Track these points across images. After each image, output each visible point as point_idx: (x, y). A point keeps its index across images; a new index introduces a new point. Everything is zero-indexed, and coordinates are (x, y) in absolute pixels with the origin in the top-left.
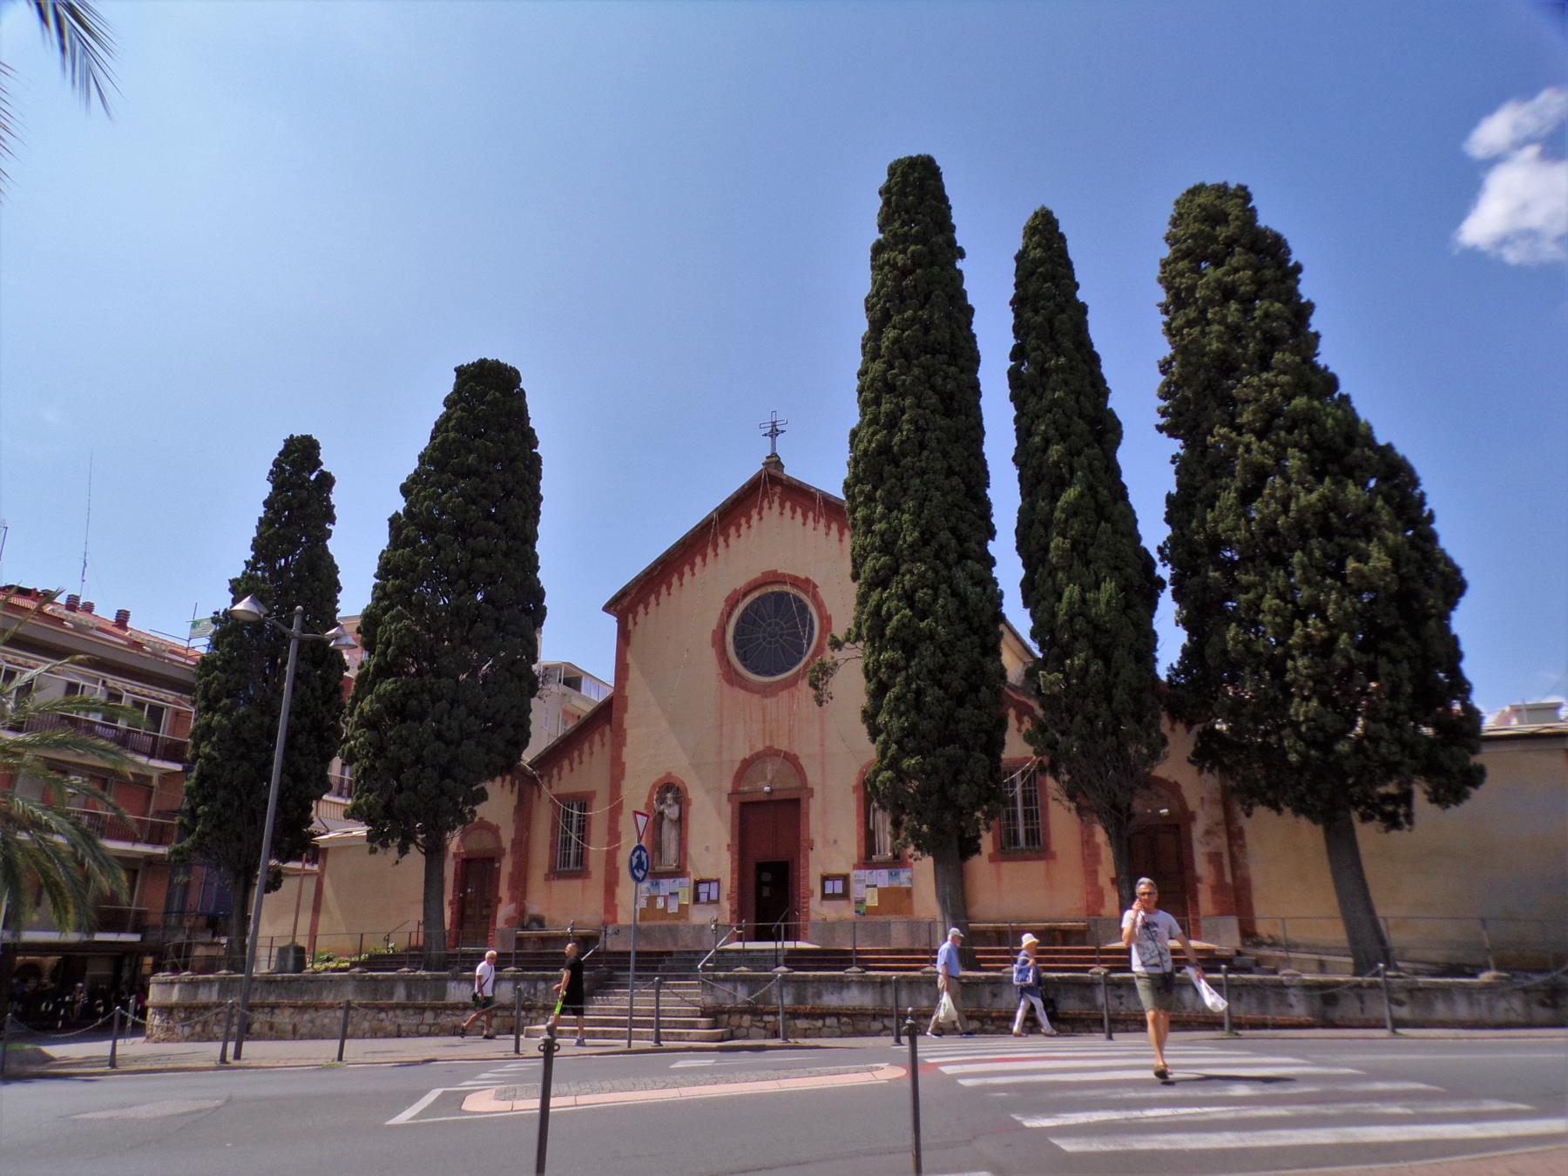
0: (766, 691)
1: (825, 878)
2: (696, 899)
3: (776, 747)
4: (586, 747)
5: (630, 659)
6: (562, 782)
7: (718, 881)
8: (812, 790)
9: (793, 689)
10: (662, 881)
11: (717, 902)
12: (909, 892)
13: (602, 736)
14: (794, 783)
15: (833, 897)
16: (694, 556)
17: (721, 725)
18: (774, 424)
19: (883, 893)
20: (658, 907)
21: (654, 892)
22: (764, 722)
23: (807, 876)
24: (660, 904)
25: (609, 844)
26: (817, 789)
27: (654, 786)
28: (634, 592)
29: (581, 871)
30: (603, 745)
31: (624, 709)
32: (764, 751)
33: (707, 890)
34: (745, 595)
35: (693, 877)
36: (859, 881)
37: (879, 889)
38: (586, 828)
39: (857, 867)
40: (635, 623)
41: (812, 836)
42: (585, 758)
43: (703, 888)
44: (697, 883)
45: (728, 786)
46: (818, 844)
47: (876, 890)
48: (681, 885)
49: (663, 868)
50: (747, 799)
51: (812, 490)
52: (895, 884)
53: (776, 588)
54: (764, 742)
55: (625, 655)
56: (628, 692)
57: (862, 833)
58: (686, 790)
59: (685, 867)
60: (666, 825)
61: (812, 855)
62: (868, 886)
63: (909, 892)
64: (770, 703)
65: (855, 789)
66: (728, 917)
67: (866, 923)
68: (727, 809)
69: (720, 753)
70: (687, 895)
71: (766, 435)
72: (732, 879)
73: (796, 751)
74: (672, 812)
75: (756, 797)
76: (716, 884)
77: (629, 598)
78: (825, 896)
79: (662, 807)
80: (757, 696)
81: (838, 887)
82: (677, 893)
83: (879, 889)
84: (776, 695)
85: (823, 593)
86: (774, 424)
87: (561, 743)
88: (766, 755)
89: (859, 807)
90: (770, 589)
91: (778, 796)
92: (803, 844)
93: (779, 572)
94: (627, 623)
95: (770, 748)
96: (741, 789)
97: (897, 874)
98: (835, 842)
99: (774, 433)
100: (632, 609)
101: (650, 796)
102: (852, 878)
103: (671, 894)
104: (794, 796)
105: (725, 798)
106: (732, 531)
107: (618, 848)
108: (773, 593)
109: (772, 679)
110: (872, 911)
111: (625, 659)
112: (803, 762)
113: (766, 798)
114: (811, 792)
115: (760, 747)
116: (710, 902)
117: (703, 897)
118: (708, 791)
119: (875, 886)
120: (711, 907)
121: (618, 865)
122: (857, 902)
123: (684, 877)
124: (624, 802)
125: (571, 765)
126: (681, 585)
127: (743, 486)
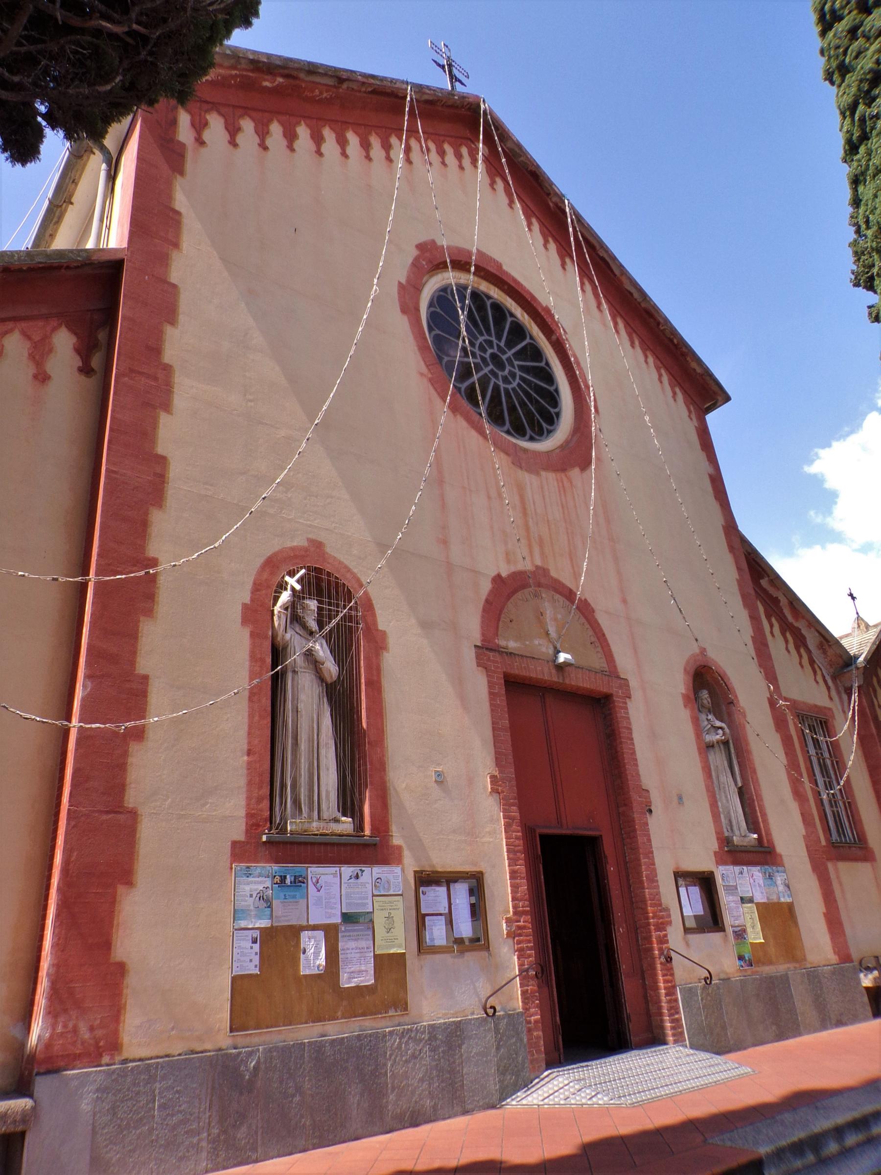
9: (563, 475)
10: (314, 871)
14: (596, 661)
20: (304, 971)
33: (443, 908)
37: (758, 905)
48: (380, 891)
50: (518, 669)
69: (445, 542)
72: (513, 875)
83: (758, 905)
98: (680, 798)
103: (348, 918)
105: (469, 655)
107: (139, 734)
113: (553, 677)
120: (471, 958)
121: (131, 799)
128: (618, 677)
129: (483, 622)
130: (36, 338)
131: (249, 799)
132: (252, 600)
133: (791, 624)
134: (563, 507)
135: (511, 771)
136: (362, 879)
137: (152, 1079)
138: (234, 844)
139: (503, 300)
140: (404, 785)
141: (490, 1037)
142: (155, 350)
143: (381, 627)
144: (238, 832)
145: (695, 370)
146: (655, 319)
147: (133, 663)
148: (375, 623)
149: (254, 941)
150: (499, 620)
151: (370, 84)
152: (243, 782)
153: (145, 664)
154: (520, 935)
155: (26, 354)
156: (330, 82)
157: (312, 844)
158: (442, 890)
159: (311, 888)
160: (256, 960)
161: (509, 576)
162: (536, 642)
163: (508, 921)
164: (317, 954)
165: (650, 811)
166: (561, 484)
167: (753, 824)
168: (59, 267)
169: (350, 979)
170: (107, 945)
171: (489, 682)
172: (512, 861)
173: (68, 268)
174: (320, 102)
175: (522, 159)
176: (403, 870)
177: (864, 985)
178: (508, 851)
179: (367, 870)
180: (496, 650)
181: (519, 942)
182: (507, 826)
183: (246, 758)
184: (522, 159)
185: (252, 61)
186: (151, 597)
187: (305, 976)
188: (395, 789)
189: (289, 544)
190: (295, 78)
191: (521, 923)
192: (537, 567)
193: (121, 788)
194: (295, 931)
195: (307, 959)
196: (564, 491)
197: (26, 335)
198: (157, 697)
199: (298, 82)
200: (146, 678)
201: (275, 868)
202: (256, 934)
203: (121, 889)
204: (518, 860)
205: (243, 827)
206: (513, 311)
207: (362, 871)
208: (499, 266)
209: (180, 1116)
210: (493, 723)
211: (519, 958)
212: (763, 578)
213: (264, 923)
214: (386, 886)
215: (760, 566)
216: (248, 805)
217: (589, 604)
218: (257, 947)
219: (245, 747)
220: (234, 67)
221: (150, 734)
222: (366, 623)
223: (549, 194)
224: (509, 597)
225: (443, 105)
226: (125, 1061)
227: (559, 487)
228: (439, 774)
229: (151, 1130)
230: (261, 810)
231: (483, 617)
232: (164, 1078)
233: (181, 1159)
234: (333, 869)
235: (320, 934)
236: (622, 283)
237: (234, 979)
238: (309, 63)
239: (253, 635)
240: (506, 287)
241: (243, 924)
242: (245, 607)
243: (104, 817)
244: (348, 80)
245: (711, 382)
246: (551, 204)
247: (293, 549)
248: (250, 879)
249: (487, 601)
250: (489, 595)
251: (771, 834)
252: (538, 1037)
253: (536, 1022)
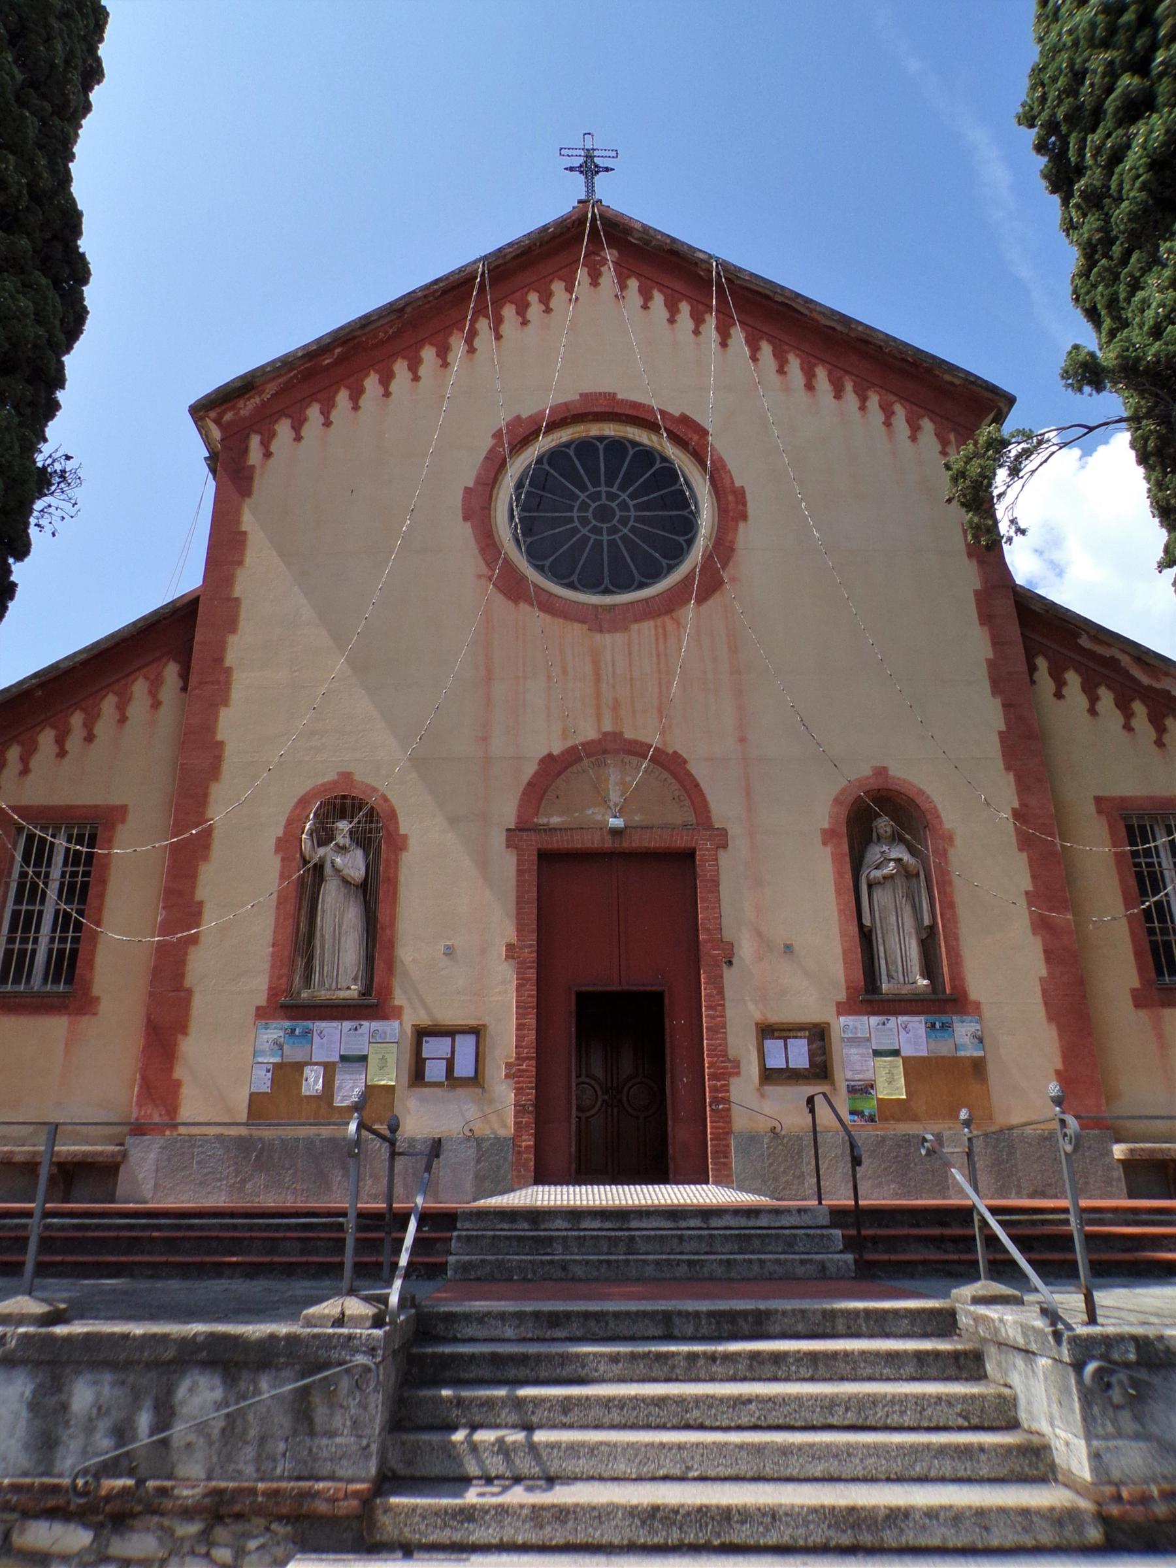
0: (597, 620)
1: (767, 1031)
2: (418, 1076)
3: (629, 735)
4: (109, 704)
5: (248, 521)
6: (31, 777)
7: (477, 1032)
8: (724, 833)
9: (667, 619)
10: (320, 1025)
11: (476, 1080)
12: (978, 1067)
13: (155, 685)
14: (679, 814)
15: (790, 1076)
16: (420, 345)
17: (489, 679)
18: (589, 156)
19: (915, 1069)
20: (305, 1091)
21: (294, 1053)
22: (598, 679)
23: (719, 1028)
24: (313, 1081)
25: (166, 928)
26: (736, 831)
27: (304, 802)
28: (271, 388)
29: (64, 995)
30: (156, 705)
31: (231, 624)
32: (599, 741)
34: (553, 426)
35: (413, 1017)
36: (854, 1041)
37: (906, 1060)
38: (92, 892)
39: (845, 1008)
40: (268, 455)
41: (727, 935)
42: (103, 727)
43: (435, 1048)
44: (422, 1033)
45: (507, 812)
46: (746, 949)
47: (899, 1062)
49: (323, 995)
50: (556, 843)
51: (701, 256)
52: (944, 1048)
53: (610, 430)
54: (599, 717)
55: (238, 513)
56: (244, 585)
57: (853, 929)
58: (393, 815)
59: (387, 992)
60: (331, 894)
61: (730, 976)
62: (877, 1053)
63: (978, 1067)
64: (610, 642)
65: (828, 836)
66: (511, 1121)
67: (883, 1140)
68: (506, 864)
69: (485, 739)
70: (392, 1059)
71: (571, 169)
72: (520, 1027)
73: (678, 744)
74: (353, 864)
75: (579, 842)
76: (471, 1039)
77: (257, 400)
78: (769, 1076)
79: (322, 851)
80: (576, 630)
81: (799, 1054)
82: (363, 1059)
83: (906, 1060)
84: (626, 629)
85: (719, 443)
86: (589, 156)
87: (41, 685)
88: (605, 752)
89: (839, 874)
90: (595, 430)
91: (637, 842)
92: (709, 951)
93: (619, 397)
94: (245, 451)
95: (616, 736)
96: (543, 820)
97: (946, 1027)
99: (589, 169)
100: (263, 423)
101: (293, 824)
102: (836, 1035)
103: (344, 1058)
104: (681, 841)
105: (498, 839)
106: (509, 311)
107: (194, 940)
108: (601, 439)
109: (608, 600)
110: (890, 1111)
111: (238, 522)
112: (698, 770)
113: (609, 844)
114: (721, 839)
115: (588, 732)
116: (452, 1079)
117: (435, 1071)
118: (453, 821)
119: (896, 1053)
121: (188, 982)
122: (852, 1090)
123: (385, 1018)
124: (216, 834)
125: (60, 741)
126: (387, 394)
127: (545, 228)
128: (711, 828)
129: (520, 806)
130: (152, 677)
131: (271, 977)
132: (285, 833)
133: (1150, 688)
134: (658, 656)
135: (532, 939)
136: (360, 1031)
137: (193, 1146)
138: (258, 1008)
139: (622, 434)
140: (411, 959)
141: (471, 1153)
142: (220, 660)
143: (402, 831)
144: (262, 1000)
145: (952, 383)
146: (874, 344)
147: (193, 894)
148: (397, 828)
149: (268, 1071)
150: (542, 799)
151: (435, 291)
152: (267, 966)
153: (201, 893)
154: (520, 1077)
155: (146, 691)
156: (393, 317)
157: (321, 1006)
158: (448, 1040)
159: (316, 1039)
160: (269, 1083)
161: (563, 753)
162: (589, 812)
163: (508, 1065)
164: (316, 1082)
165: (730, 963)
166: (660, 630)
167: (930, 967)
168: (158, 622)
169: (342, 1101)
170: (170, 1070)
171: (518, 860)
172: (520, 1016)
173: (164, 619)
174: (390, 339)
175: (653, 243)
176: (401, 1024)
177: (1116, 1157)
178: (517, 1007)
179: (366, 1023)
180: (536, 829)
181: (517, 1083)
182: (519, 987)
183: (271, 949)
184: (653, 243)
185: (303, 356)
186: (207, 847)
187: (307, 1097)
188: (402, 962)
189: (321, 781)
190: (355, 338)
191: (524, 1067)
192: (605, 734)
193: (182, 976)
194: (299, 1067)
195: (308, 1085)
196: (665, 635)
197: (146, 678)
198: (207, 914)
199: (356, 341)
200: (201, 903)
201: (287, 1024)
202: (270, 1066)
203: (180, 1037)
204: (530, 1014)
205: (266, 996)
206: (637, 439)
207: (361, 1025)
208: (611, 397)
209: (210, 1170)
210: (518, 897)
211: (515, 1095)
212: (1078, 636)
213: (277, 1060)
214: (383, 1036)
215: (1067, 621)
216: (270, 981)
217: (680, 756)
218: (269, 1075)
219: (271, 942)
220: (291, 370)
221: (203, 939)
222: (388, 831)
223: (696, 264)
224: (559, 774)
225: (541, 245)
226: (180, 1135)
227: (656, 635)
228: (448, 947)
229: (190, 1174)
230: (281, 984)
231: (521, 800)
232: (201, 1146)
233: (209, 1193)
234: (335, 1024)
235: (321, 1070)
236: (817, 321)
237: (252, 1095)
238: (360, 318)
239: (283, 860)
240: (624, 418)
241: (260, 1060)
242: (279, 840)
243: (170, 994)
244: (407, 305)
245: (979, 390)
246: (702, 273)
247: (322, 785)
248: (268, 1031)
249: (530, 784)
250: (534, 776)
251: (962, 979)
252: (528, 1160)
253: (526, 1147)
